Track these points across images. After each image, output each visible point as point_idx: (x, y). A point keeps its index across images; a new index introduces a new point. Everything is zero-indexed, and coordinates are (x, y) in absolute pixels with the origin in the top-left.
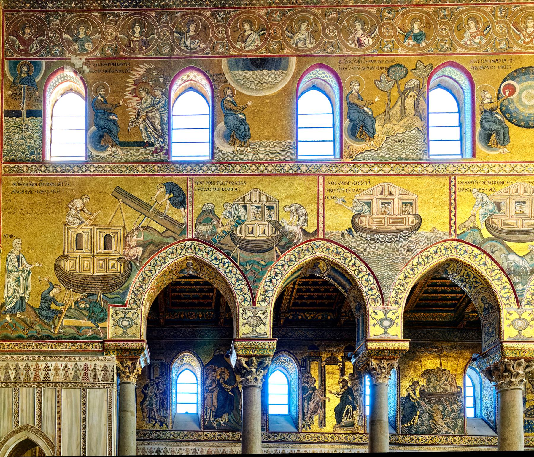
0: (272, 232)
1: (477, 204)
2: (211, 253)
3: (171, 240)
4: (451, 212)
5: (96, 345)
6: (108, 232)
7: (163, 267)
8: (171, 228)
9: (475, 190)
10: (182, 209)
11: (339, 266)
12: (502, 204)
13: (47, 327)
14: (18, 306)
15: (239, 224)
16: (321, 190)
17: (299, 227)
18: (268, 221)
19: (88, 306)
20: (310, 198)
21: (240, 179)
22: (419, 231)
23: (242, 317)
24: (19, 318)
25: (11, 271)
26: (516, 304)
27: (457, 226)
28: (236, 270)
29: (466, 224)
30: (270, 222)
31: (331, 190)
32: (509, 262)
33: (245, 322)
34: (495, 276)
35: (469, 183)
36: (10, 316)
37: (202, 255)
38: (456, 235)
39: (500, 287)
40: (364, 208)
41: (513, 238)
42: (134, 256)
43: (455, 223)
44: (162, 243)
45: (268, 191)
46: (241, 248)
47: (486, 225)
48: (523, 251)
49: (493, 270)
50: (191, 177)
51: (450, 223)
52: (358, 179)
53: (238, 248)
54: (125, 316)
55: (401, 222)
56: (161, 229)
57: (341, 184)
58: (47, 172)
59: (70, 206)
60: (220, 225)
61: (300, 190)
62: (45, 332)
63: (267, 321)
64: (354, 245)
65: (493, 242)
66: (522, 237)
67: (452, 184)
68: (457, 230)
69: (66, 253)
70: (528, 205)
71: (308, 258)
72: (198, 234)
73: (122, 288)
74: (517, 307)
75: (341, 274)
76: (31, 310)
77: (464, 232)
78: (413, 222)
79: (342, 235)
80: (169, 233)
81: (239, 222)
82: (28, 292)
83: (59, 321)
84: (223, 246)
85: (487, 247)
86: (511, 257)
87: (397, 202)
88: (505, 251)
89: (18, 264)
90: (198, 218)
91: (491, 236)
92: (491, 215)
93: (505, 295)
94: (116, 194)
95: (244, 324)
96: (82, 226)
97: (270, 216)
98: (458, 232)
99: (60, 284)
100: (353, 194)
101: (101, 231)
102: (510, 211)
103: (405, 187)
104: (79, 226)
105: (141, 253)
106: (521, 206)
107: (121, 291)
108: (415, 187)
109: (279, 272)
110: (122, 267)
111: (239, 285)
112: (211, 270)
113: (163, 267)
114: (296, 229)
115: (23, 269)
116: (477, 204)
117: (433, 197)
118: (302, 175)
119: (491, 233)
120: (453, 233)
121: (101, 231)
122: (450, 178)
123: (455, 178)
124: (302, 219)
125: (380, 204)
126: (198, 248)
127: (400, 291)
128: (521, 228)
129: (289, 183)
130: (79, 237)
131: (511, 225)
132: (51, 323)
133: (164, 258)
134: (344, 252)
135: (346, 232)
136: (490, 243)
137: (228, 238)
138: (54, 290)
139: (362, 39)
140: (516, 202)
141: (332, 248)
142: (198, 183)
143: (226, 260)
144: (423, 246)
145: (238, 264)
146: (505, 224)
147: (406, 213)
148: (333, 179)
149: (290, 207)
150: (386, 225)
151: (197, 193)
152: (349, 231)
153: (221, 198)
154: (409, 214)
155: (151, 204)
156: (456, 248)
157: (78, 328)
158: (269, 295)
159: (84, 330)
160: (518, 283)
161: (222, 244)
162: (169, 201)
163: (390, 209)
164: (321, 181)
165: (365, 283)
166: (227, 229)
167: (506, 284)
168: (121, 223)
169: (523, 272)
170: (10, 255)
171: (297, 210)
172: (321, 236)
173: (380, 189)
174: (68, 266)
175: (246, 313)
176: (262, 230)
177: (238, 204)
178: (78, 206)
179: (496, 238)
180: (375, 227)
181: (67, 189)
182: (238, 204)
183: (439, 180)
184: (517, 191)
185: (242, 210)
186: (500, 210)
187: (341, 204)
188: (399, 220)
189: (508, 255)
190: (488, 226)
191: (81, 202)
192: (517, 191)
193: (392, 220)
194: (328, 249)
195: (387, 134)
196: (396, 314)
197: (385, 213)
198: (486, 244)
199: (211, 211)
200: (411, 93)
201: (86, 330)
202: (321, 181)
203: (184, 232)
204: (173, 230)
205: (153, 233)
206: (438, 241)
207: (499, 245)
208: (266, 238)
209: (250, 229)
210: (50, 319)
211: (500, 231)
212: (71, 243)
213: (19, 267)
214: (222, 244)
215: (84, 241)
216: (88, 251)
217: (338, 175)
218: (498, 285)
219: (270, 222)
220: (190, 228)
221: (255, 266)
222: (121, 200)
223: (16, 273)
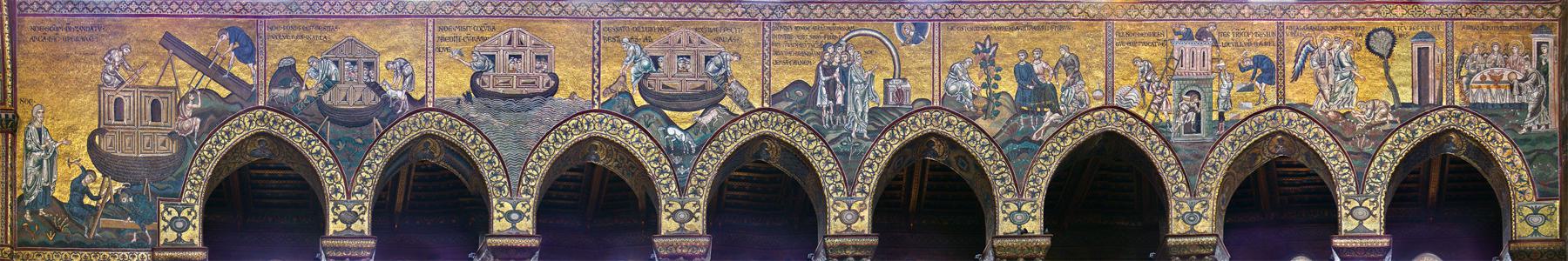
0: (371, 98)
1: (628, 59)
2: (291, 127)
3: (237, 108)
4: (594, 71)
5: (143, 256)
6: (154, 96)
7: (227, 145)
8: (237, 90)
9: (625, 40)
10: (251, 65)
11: (454, 143)
13: (79, 230)
14: (40, 200)
15: (330, 87)
16: (430, 38)
17: (404, 91)
18: (366, 83)
19: (131, 200)
20: (417, 50)
21: (330, 23)
22: (556, 96)
23: (333, 211)
24: (43, 216)
25: (31, 151)
27: (602, 91)
28: (324, 151)
29: (613, 88)
30: (369, 84)
31: (443, 39)
33: (336, 217)
34: (651, 156)
35: (617, 30)
36: (31, 214)
37: (278, 129)
39: (657, 171)
42: (189, 129)
44: (226, 112)
45: (366, 40)
46: (333, 122)
47: (639, 89)
48: (686, 123)
49: (648, 149)
50: (263, 20)
52: (478, 23)
53: (328, 120)
54: (179, 214)
55: (534, 83)
56: (224, 92)
57: (457, 30)
58: (75, 12)
59: (106, 59)
60: (304, 88)
61: (405, 39)
62: (76, 237)
63: (366, 217)
64: (474, 116)
65: (650, 112)
66: (685, 104)
69: (101, 127)
70: (692, 61)
71: (412, 133)
72: (273, 100)
73: (174, 175)
75: (458, 155)
76: (58, 205)
77: (610, 99)
78: (548, 84)
79: (458, 103)
80: (236, 98)
81: (328, 85)
82: (54, 180)
83: (94, 222)
84: (308, 117)
86: (671, 131)
88: (665, 125)
89: (40, 140)
90: (273, 78)
91: (645, 103)
92: (646, 76)
93: (664, 182)
94: (165, 42)
95: (335, 221)
96: (122, 88)
97: (368, 75)
98: (603, 100)
99: (95, 169)
100: (472, 44)
101: (147, 94)
102: (671, 69)
103: (540, 34)
104: (118, 87)
105: (198, 126)
107: (174, 180)
108: (551, 35)
109: (380, 154)
110: (174, 146)
111: (329, 170)
112: (291, 150)
113: (227, 145)
114: (401, 95)
115: (46, 147)
116: (628, 59)
117: (572, 50)
118: (408, 16)
121: (147, 94)
123: (599, 23)
124: (407, 80)
125: (508, 58)
126: (273, 119)
127: (532, 177)
128: (684, 92)
129: (392, 28)
130: (118, 102)
132: (84, 224)
133: (228, 133)
134: (461, 125)
135: (462, 97)
137: (314, 106)
138: (88, 178)
140: (678, 57)
141: (444, 121)
142: (271, 29)
143: (311, 137)
144: (558, 118)
145: (328, 143)
146: (665, 87)
148: (447, 23)
149: (393, 63)
150: (514, 87)
151: (271, 42)
152: (467, 97)
153: (304, 49)
154: (544, 72)
155: (210, 58)
156: (601, 122)
157: (119, 231)
158: (368, 185)
159: (127, 234)
160: (680, 165)
161: (306, 115)
162: (233, 53)
164: (430, 24)
166: (314, 94)
168: (172, 83)
170: (29, 128)
171: (401, 68)
172: (430, 106)
173: (507, 37)
174: (104, 144)
175: (338, 208)
176: (358, 96)
177: (327, 58)
178: (117, 59)
179: (652, 106)
180: (500, 90)
181: (103, 36)
182: (327, 58)
185: (333, 67)
186: (657, 66)
187: (457, 58)
188: (532, 81)
190: (643, 91)
191: (121, 53)
192: (679, 42)
194: (440, 122)
196: (527, 206)
197: (514, 70)
198: (640, 115)
199: (292, 68)
201: (130, 234)
202: (430, 24)
203: (255, 95)
204: (239, 94)
205: (213, 98)
207: (656, 116)
208: (363, 107)
209: (343, 94)
210: (82, 218)
211: (659, 96)
212: (109, 113)
213: (41, 144)
214: (306, 115)
215: (125, 108)
216: (131, 122)
217: (453, 16)
218: (655, 169)
219: (369, 84)
220: (261, 92)
221: (351, 146)
222: (171, 51)
223: (38, 154)
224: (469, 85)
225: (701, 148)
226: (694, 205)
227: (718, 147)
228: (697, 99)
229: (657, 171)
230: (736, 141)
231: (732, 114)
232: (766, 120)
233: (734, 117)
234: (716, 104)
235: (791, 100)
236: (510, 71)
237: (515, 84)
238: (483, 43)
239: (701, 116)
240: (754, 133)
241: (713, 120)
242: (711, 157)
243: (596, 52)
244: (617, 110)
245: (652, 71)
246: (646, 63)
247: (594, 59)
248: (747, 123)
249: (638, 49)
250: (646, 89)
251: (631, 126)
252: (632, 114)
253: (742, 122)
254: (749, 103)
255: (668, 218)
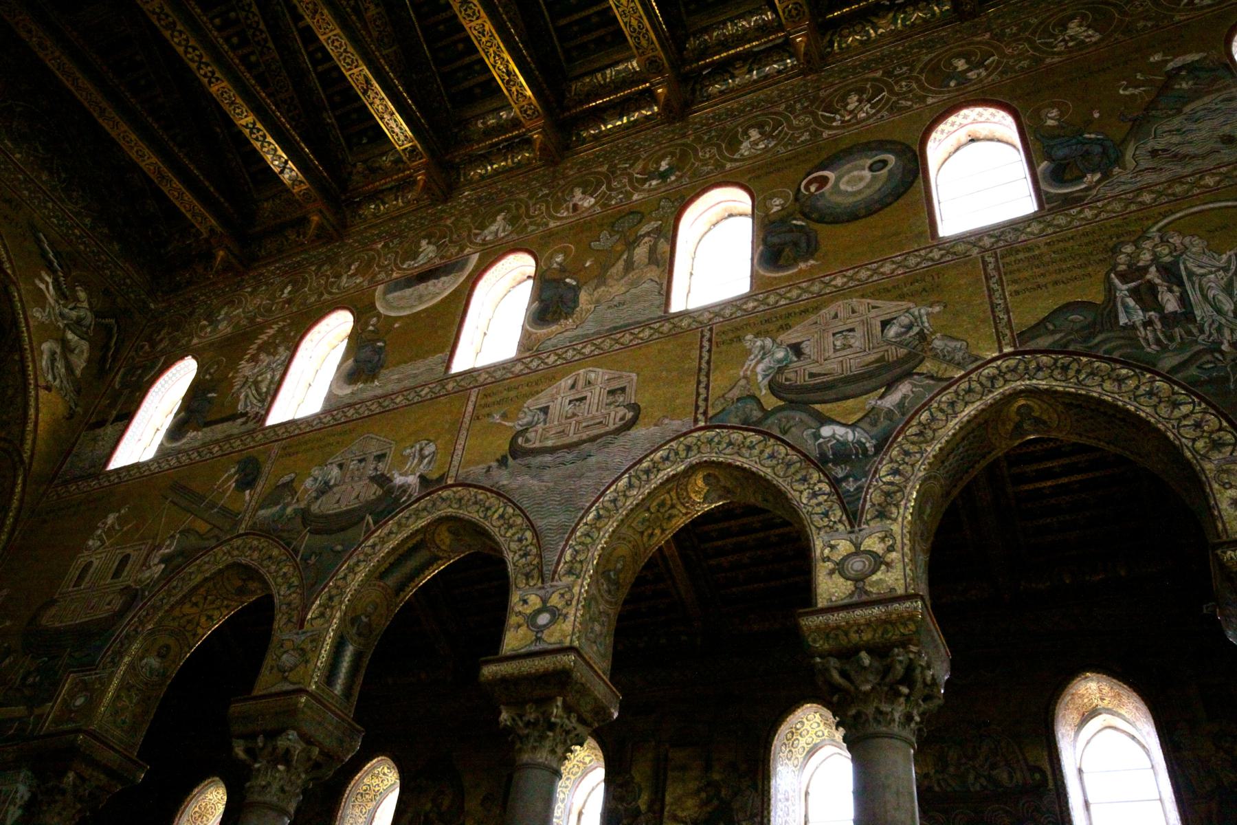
1: (752, 357)
4: (699, 382)
6: (128, 551)
12: (803, 345)
26: (846, 523)
29: (730, 395)
30: (372, 479)
32: (821, 440)
38: (706, 418)
39: (805, 494)
40: (536, 418)
41: (831, 394)
43: (706, 400)
48: (855, 413)
51: (697, 401)
55: (601, 422)
64: (505, 482)
65: (786, 413)
66: (850, 389)
67: (705, 339)
68: (710, 409)
70: (858, 333)
74: (848, 528)
78: (622, 419)
85: (773, 423)
86: (826, 431)
87: (597, 393)
92: (780, 370)
98: (711, 413)
106: (845, 337)
119: (781, 398)
120: (700, 417)
122: (702, 331)
123: (711, 330)
124: (426, 461)
131: (825, 375)
135: (494, 464)
136: (779, 415)
139: (580, 203)
140: (834, 335)
146: (812, 375)
147: (612, 407)
160: (845, 478)
163: (584, 406)
165: (514, 546)
167: (820, 485)
169: (857, 455)
172: (450, 482)
173: (570, 382)
179: (793, 405)
180: (549, 443)
183: (681, 340)
184: (836, 316)
188: (598, 421)
189: (818, 429)
192: (836, 316)
193: (584, 424)
195: (598, 302)
197: (574, 415)
200: (646, 239)
206: (668, 438)
207: (798, 416)
224: (507, 447)
225: (882, 444)
226: (882, 540)
227: (921, 434)
228: (871, 377)
229: (805, 494)
230: (955, 414)
231: (941, 380)
232: (1014, 370)
233: (945, 384)
234: (908, 374)
235: (1061, 331)
236: (567, 418)
237: (572, 431)
238: (537, 396)
239: (882, 397)
240: (991, 395)
241: (905, 397)
242: (907, 453)
243: (704, 361)
244: (734, 421)
245: (791, 362)
246: (780, 354)
247: (700, 369)
248: (974, 385)
249: (768, 342)
250: (781, 386)
251: (760, 438)
252: (760, 422)
253: (964, 385)
254: (973, 356)
255: (831, 572)
